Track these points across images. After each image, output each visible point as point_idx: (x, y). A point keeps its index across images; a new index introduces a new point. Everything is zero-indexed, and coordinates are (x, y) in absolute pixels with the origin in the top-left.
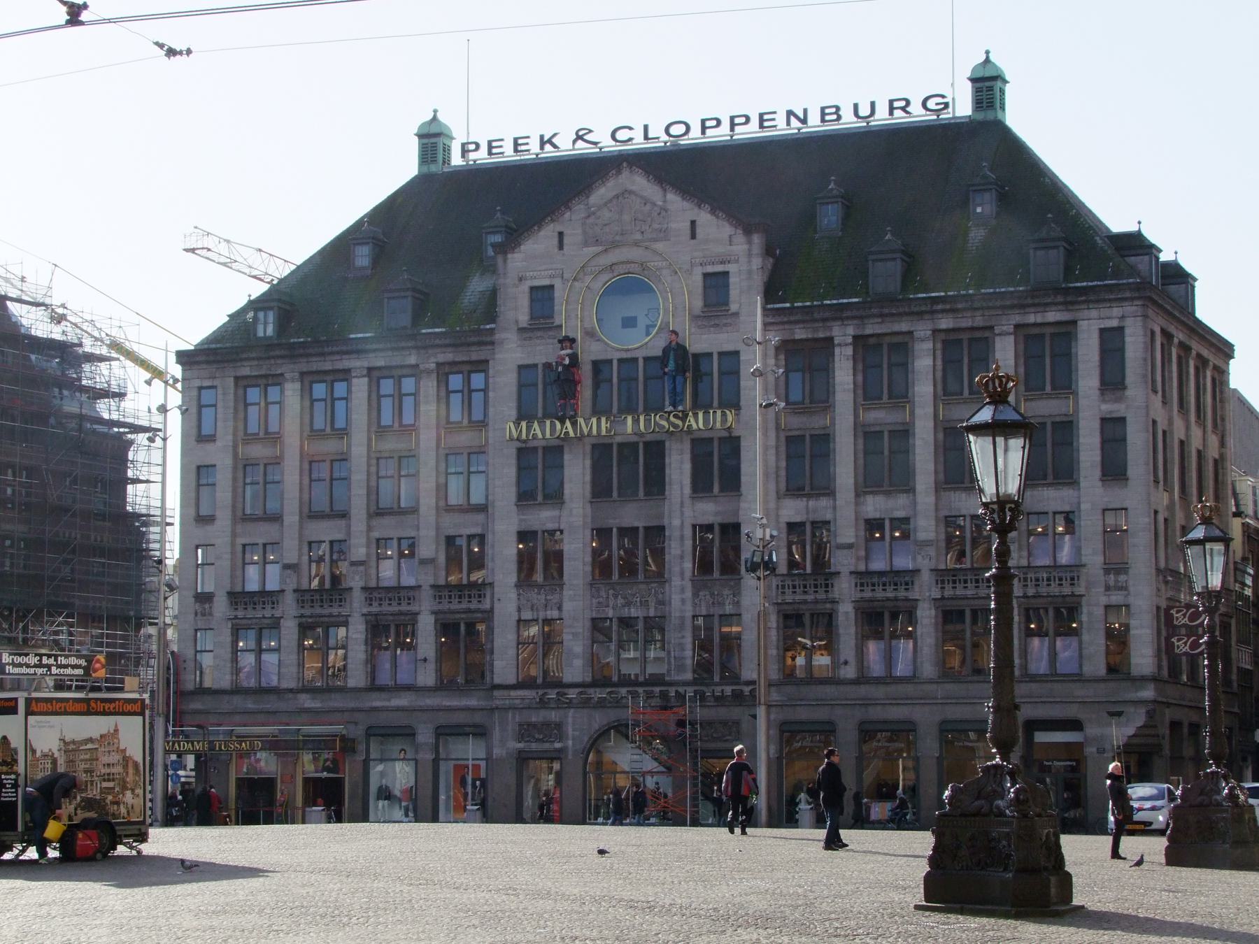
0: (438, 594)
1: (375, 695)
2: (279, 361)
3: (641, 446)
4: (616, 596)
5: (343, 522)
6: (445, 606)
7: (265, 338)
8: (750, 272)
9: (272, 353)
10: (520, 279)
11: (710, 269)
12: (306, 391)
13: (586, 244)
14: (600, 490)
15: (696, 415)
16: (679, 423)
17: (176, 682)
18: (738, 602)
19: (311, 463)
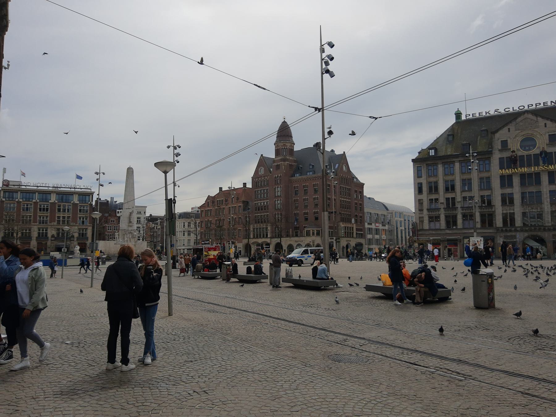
3: (534, 174)
4: (529, 207)
5: (454, 193)
6: (483, 210)
7: (432, 156)
10: (498, 139)
12: (444, 166)
13: (516, 130)
14: (522, 184)
15: (551, 166)
16: (547, 168)
17: (417, 228)
19: (445, 181)
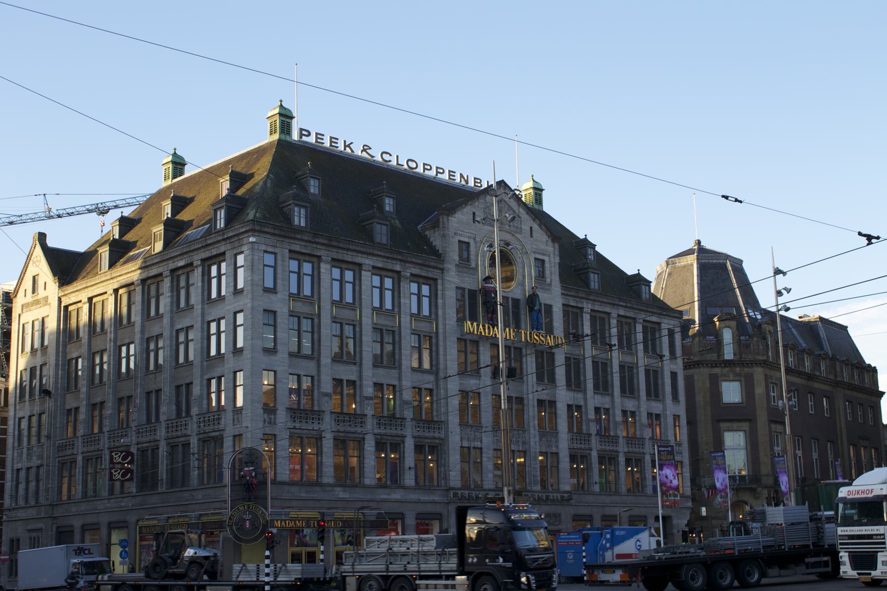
0: (417, 425)
1: (382, 490)
2: (319, 246)
8: (555, 263)
9: (317, 240)
11: (538, 256)
15: (550, 337)
18: (558, 446)
